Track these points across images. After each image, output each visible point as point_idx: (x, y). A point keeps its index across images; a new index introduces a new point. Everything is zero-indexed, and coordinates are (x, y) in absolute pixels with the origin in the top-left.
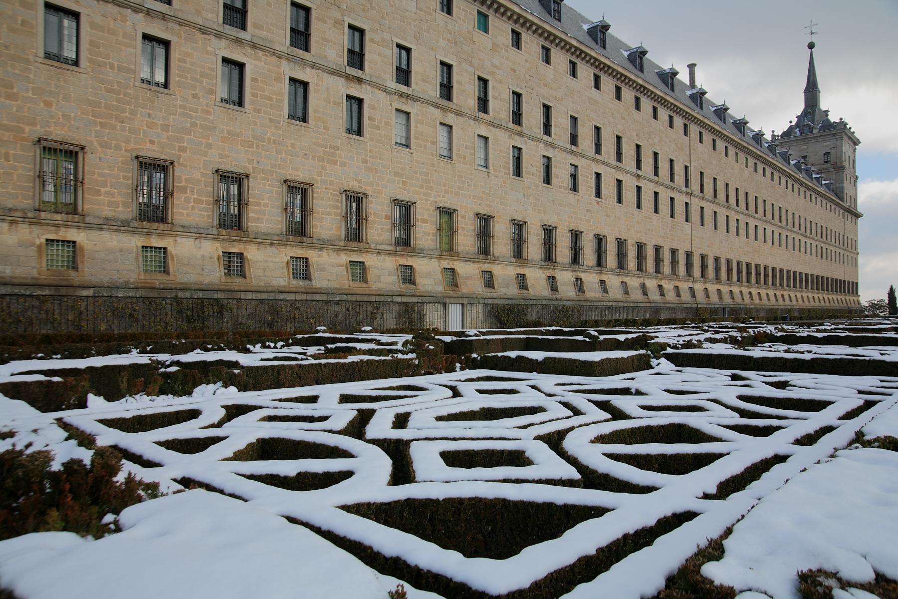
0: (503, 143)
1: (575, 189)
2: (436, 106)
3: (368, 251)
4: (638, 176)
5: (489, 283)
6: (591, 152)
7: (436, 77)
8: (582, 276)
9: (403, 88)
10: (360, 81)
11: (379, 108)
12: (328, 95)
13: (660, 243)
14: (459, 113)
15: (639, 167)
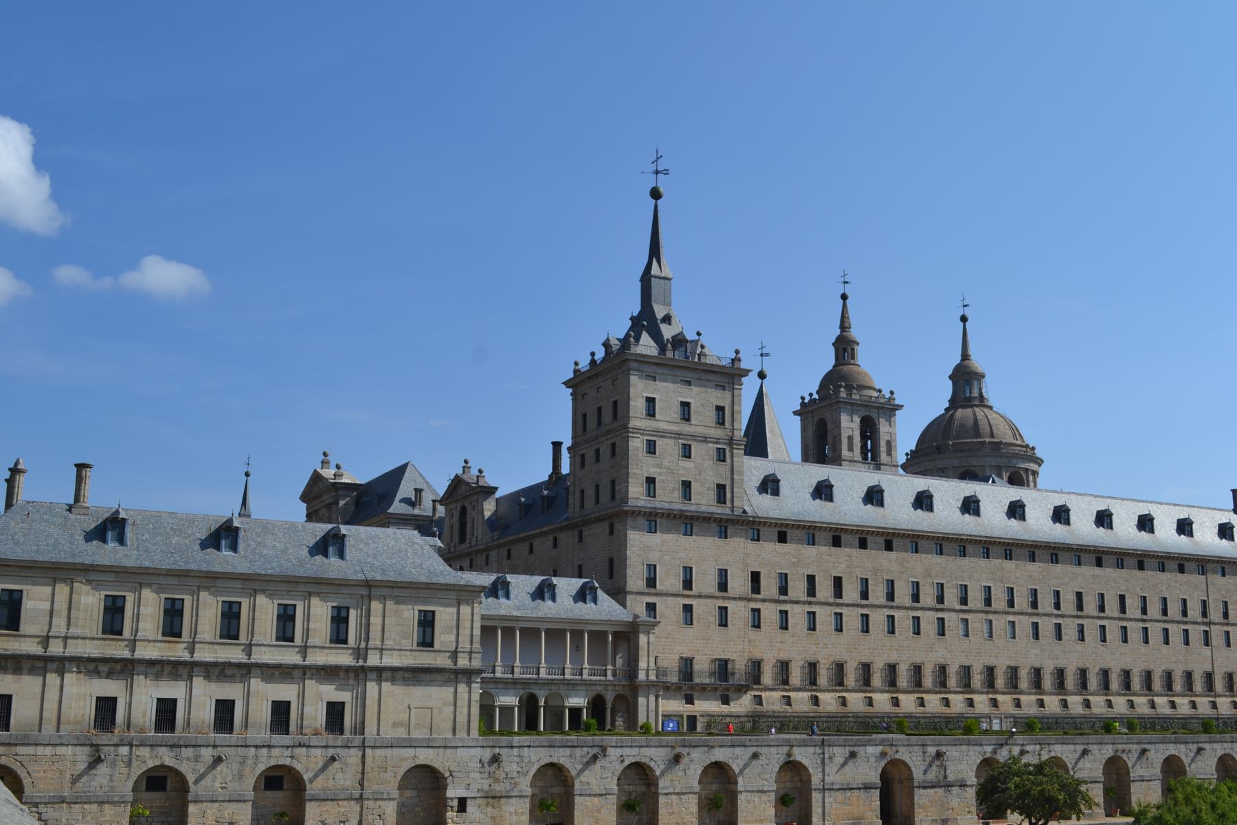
0: (1024, 624)
1: (1082, 639)
2: (982, 612)
3: (950, 692)
4: (1144, 621)
5: (1018, 704)
6: (1096, 613)
7: (981, 596)
8: (1090, 698)
9: (964, 607)
10: (942, 610)
11: (952, 619)
12: (928, 620)
13: (1171, 667)
14: (995, 612)
15: (1144, 611)
